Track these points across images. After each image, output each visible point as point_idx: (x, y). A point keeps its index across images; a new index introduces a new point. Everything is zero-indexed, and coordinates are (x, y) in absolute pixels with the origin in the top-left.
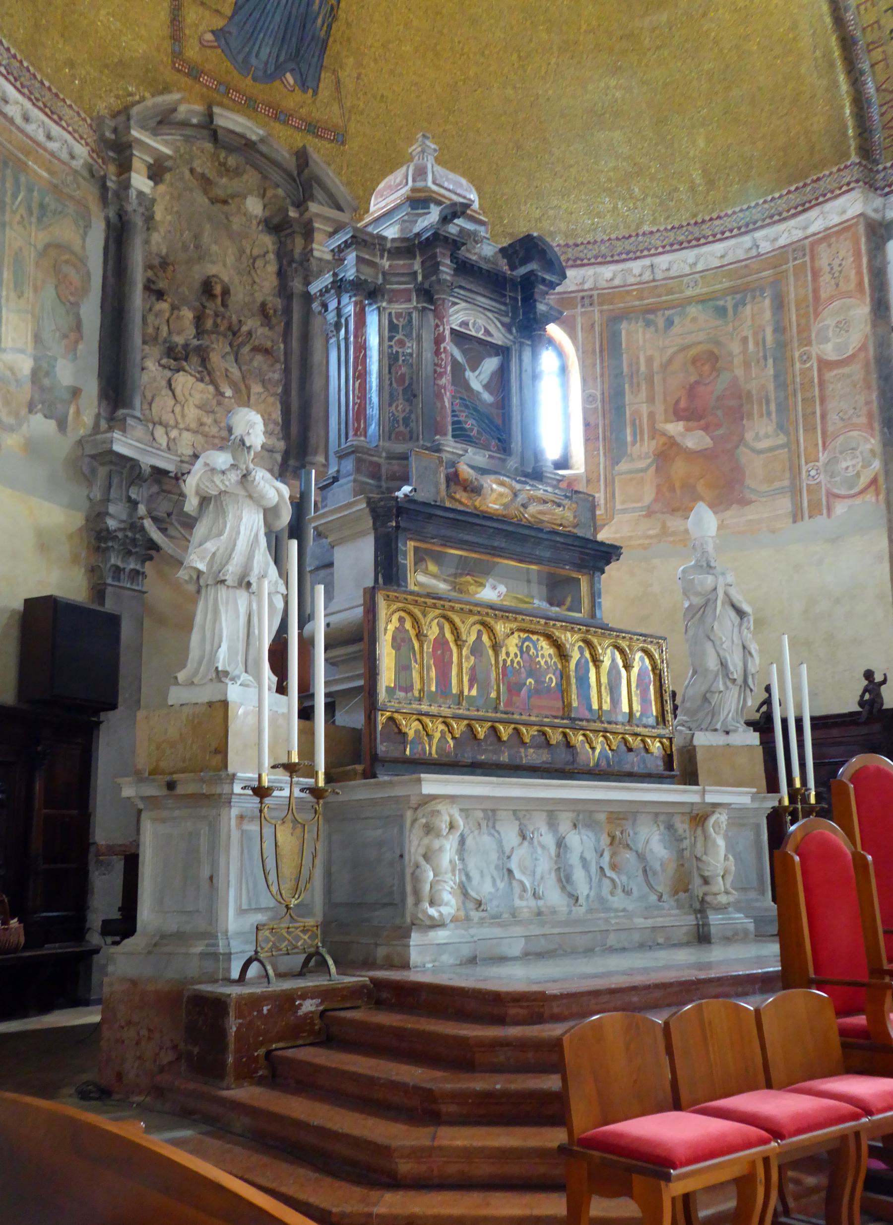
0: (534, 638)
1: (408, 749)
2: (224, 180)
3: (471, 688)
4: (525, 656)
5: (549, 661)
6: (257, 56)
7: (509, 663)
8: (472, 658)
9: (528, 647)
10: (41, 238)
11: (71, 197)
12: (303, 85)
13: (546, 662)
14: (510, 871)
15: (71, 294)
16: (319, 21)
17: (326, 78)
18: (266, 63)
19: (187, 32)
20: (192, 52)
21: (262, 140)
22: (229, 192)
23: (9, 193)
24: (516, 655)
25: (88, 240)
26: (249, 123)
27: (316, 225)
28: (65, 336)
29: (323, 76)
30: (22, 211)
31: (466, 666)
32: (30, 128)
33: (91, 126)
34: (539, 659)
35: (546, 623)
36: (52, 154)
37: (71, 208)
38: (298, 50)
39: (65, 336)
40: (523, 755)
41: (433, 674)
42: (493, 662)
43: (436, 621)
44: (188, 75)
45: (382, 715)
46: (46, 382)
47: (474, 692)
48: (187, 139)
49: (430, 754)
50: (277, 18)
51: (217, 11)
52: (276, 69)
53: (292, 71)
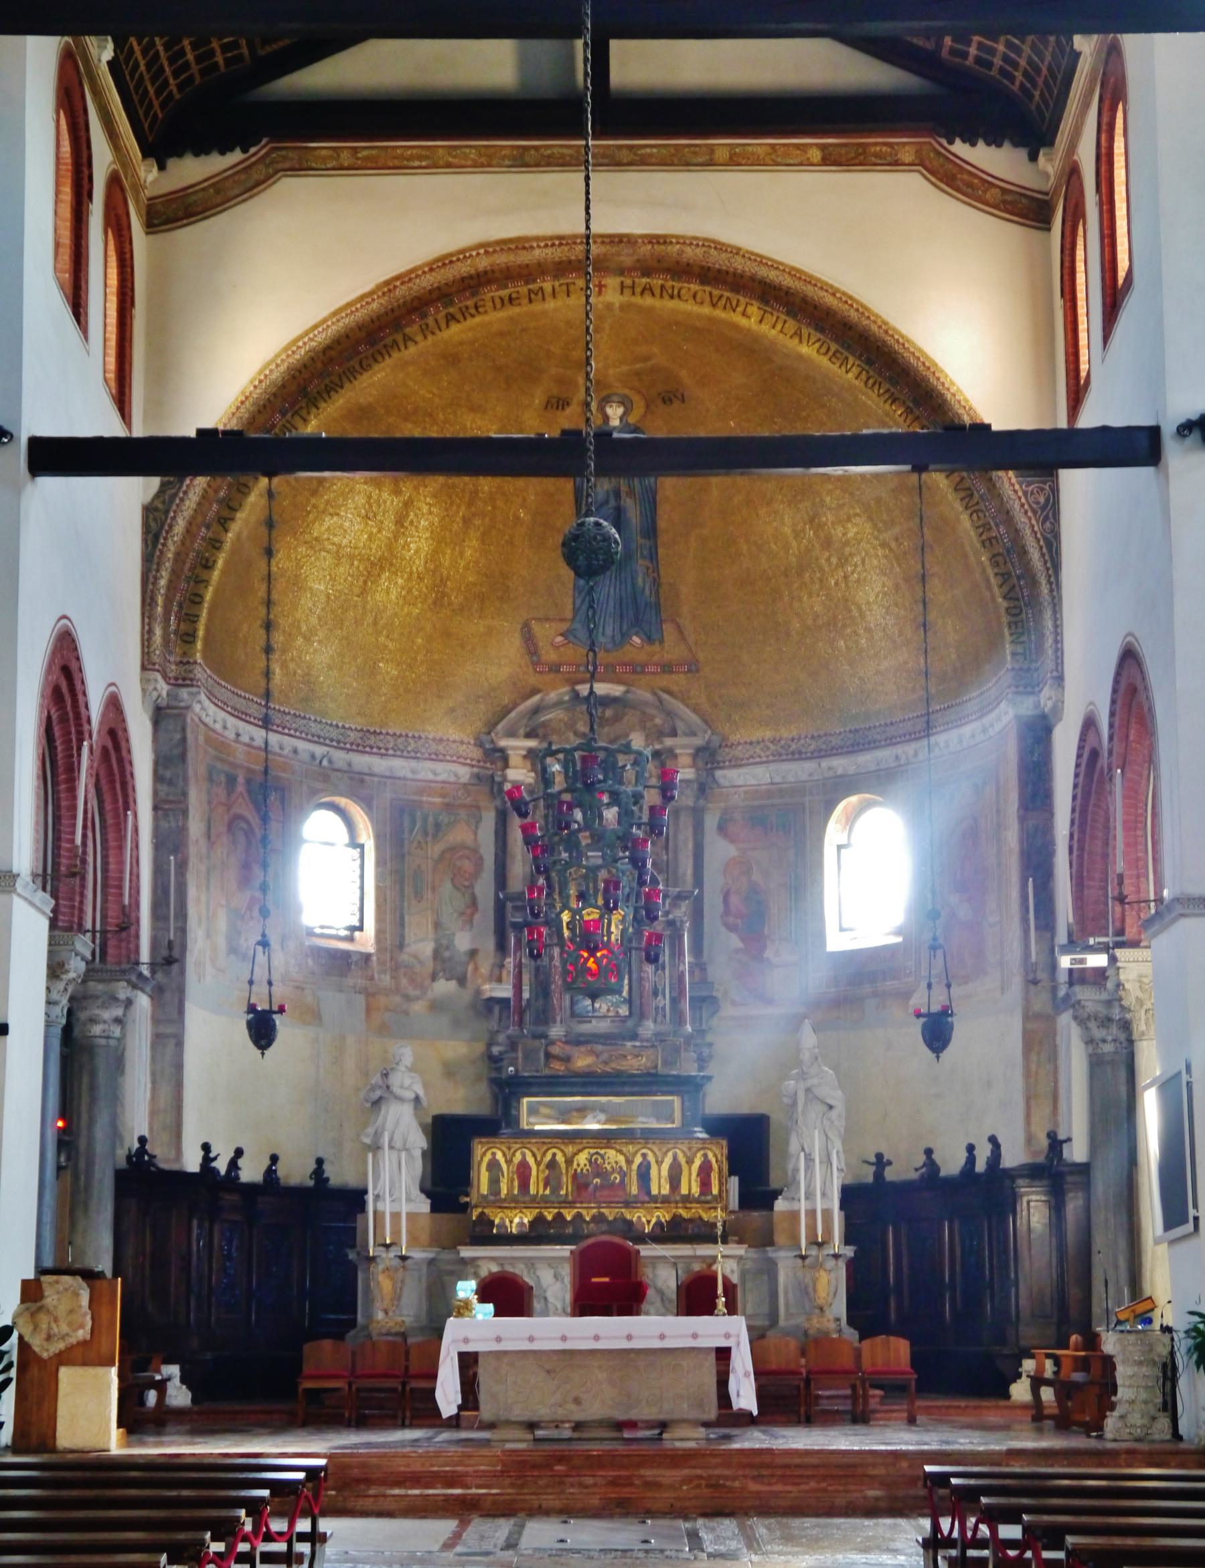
0: (602, 1152)
2: (606, 729)
3: (545, 1188)
6: (603, 634)
9: (596, 1160)
10: (435, 850)
11: (463, 806)
12: (649, 639)
14: (546, 1299)
15: (466, 880)
16: (647, 592)
17: (668, 628)
18: (613, 636)
19: (541, 644)
20: (551, 656)
21: (627, 692)
22: (612, 736)
23: (406, 830)
25: (480, 832)
26: (609, 686)
27: (678, 751)
28: (462, 914)
29: (664, 627)
30: (420, 838)
31: (542, 1176)
32: (420, 776)
33: (475, 745)
36: (444, 782)
37: (463, 814)
38: (637, 619)
39: (462, 914)
41: (516, 1183)
44: (550, 670)
46: (447, 954)
47: (548, 1192)
48: (566, 709)
50: (611, 603)
51: (562, 620)
52: (623, 635)
53: (637, 634)
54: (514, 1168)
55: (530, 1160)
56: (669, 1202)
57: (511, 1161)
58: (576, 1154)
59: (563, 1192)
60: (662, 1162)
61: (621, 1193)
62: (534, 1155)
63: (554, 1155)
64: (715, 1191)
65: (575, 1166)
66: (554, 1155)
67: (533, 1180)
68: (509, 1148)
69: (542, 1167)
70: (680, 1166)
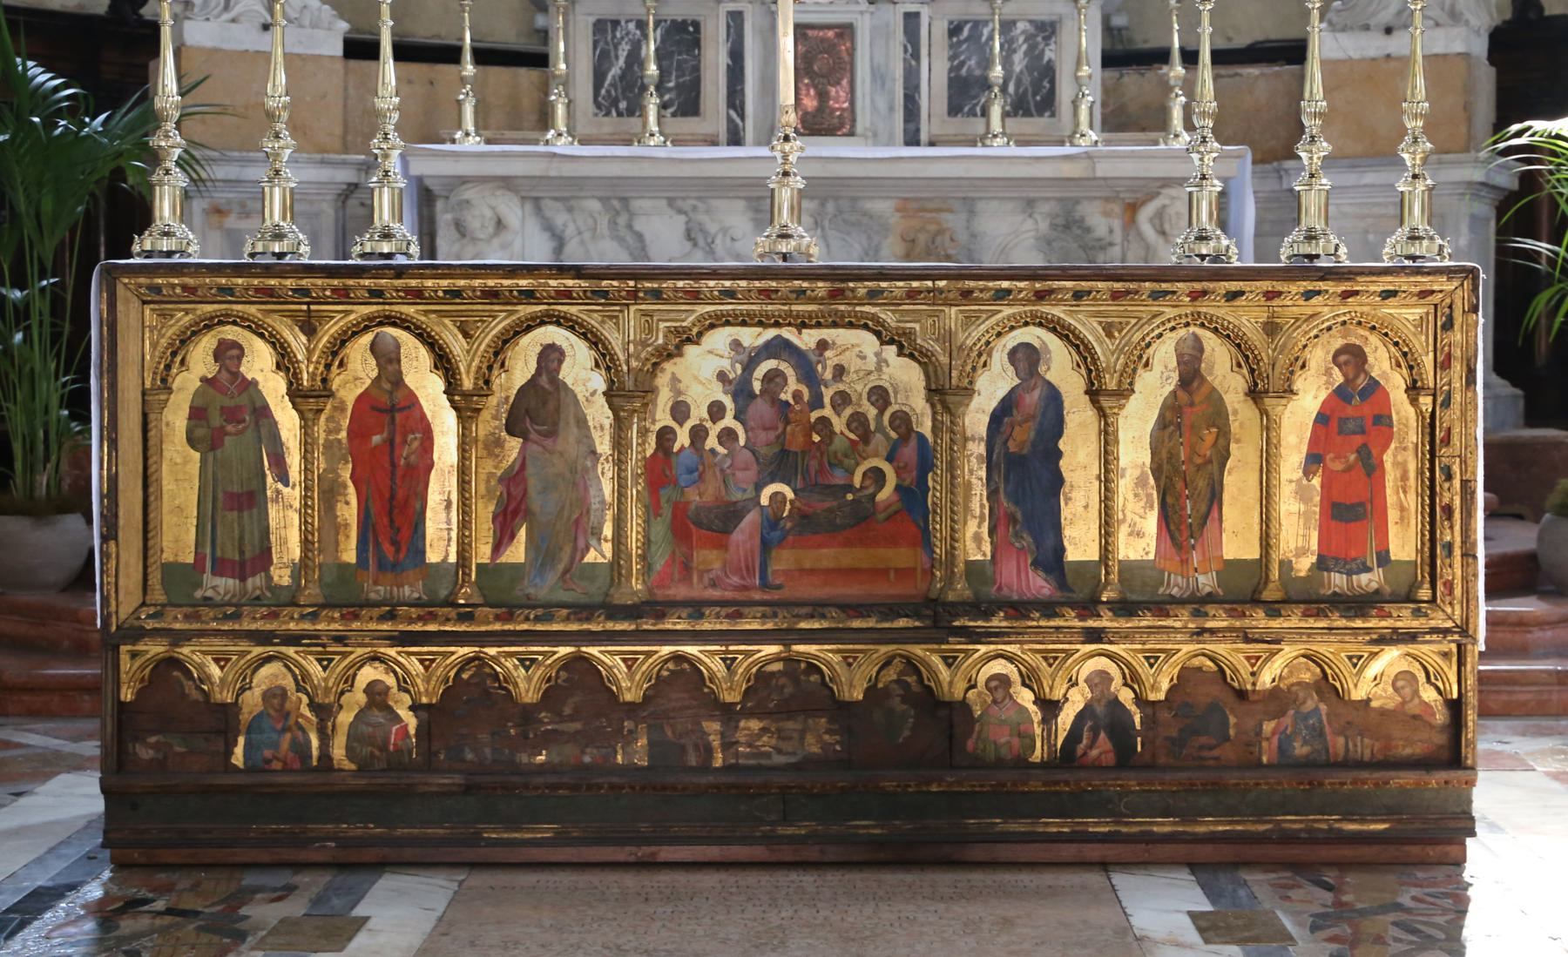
0: (807, 340)
1: (239, 751)
3: (503, 539)
4: (761, 409)
5: (872, 412)
7: (683, 438)
8: (514, 445)
13: (858, 421)
24: (716, 411)
31: (486, 470)
34: (827, 411)
35: (835, 295)
40: (716, 742)
41: (349, 511)
42: (604, 446)
43: (367, 339)
45: (134, 655)
47: (516, 553)
49: (325, 756)
54: (336, 426)
55: (428, 387)
56: (1162, 607)
57: (324, 391)
58: (668, 354)
59: (599, 554)
60: (1124, 393)
61: (901, 556)
62: (443, 362)
63: (551, 356)
64: (1403, 544)
65: (663, 418)
66: (551, 356)
67: (441, 488)
68: (309, 329)
69: (489, 423)
70: (1218, 417)
